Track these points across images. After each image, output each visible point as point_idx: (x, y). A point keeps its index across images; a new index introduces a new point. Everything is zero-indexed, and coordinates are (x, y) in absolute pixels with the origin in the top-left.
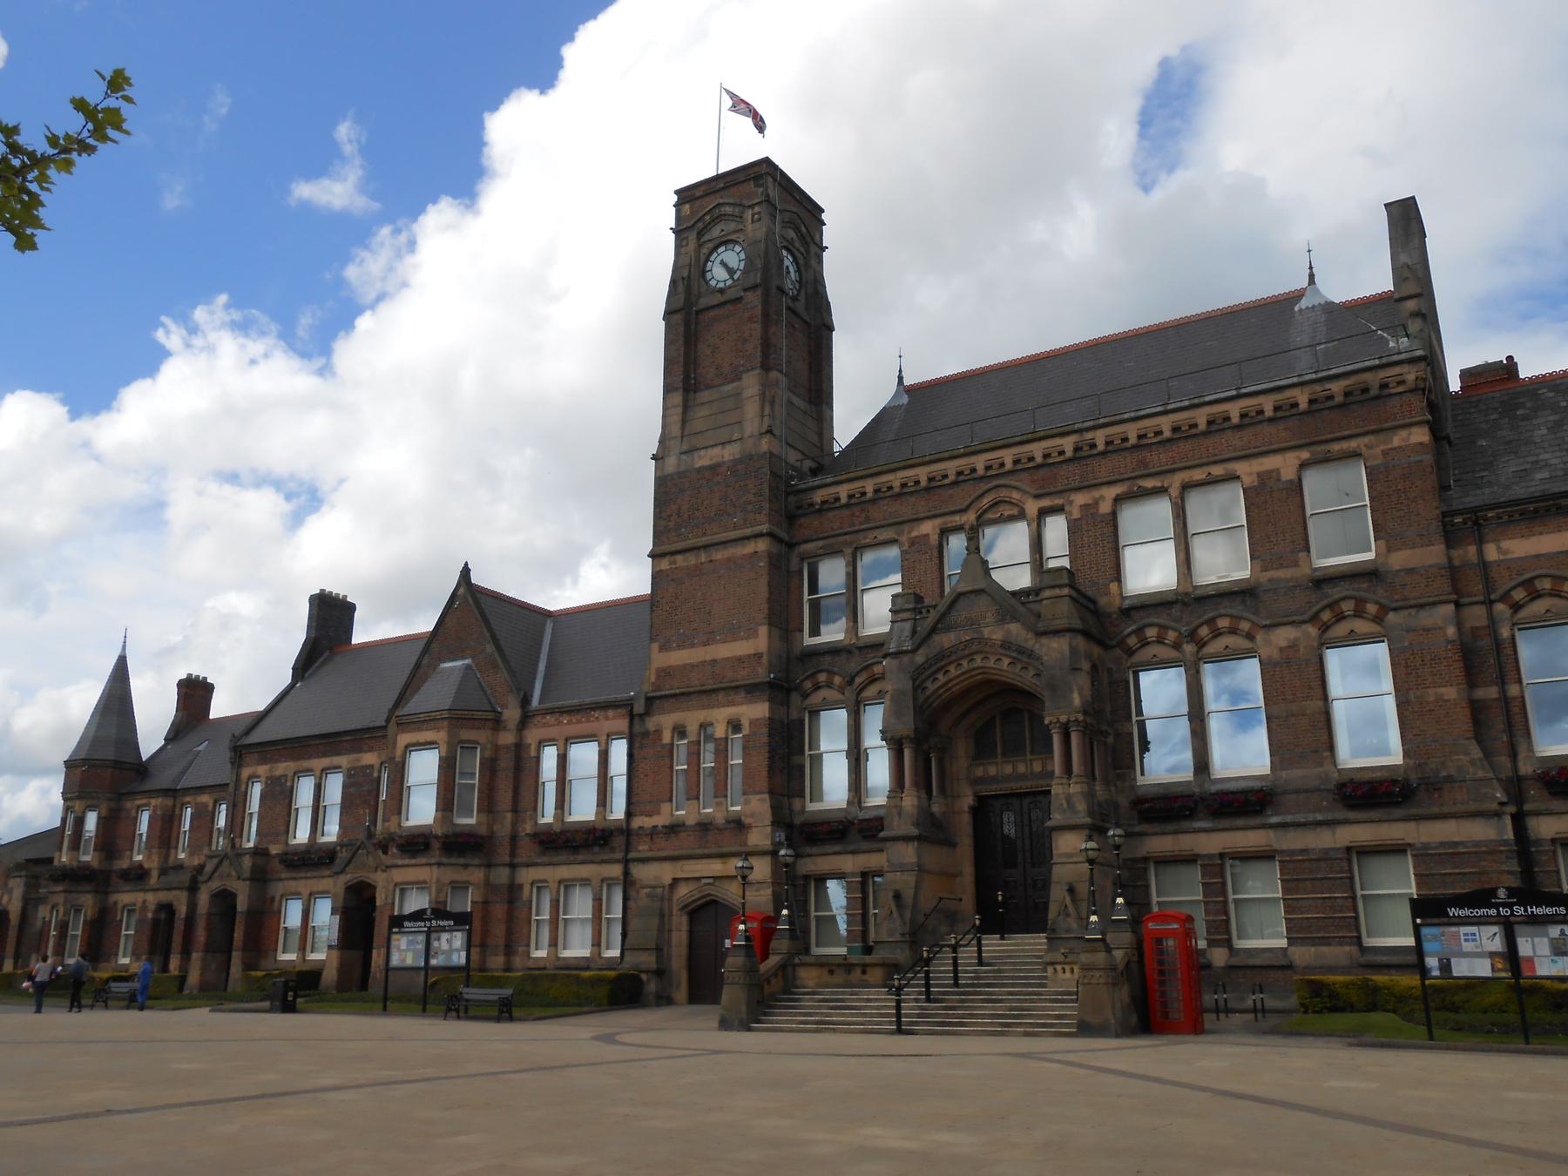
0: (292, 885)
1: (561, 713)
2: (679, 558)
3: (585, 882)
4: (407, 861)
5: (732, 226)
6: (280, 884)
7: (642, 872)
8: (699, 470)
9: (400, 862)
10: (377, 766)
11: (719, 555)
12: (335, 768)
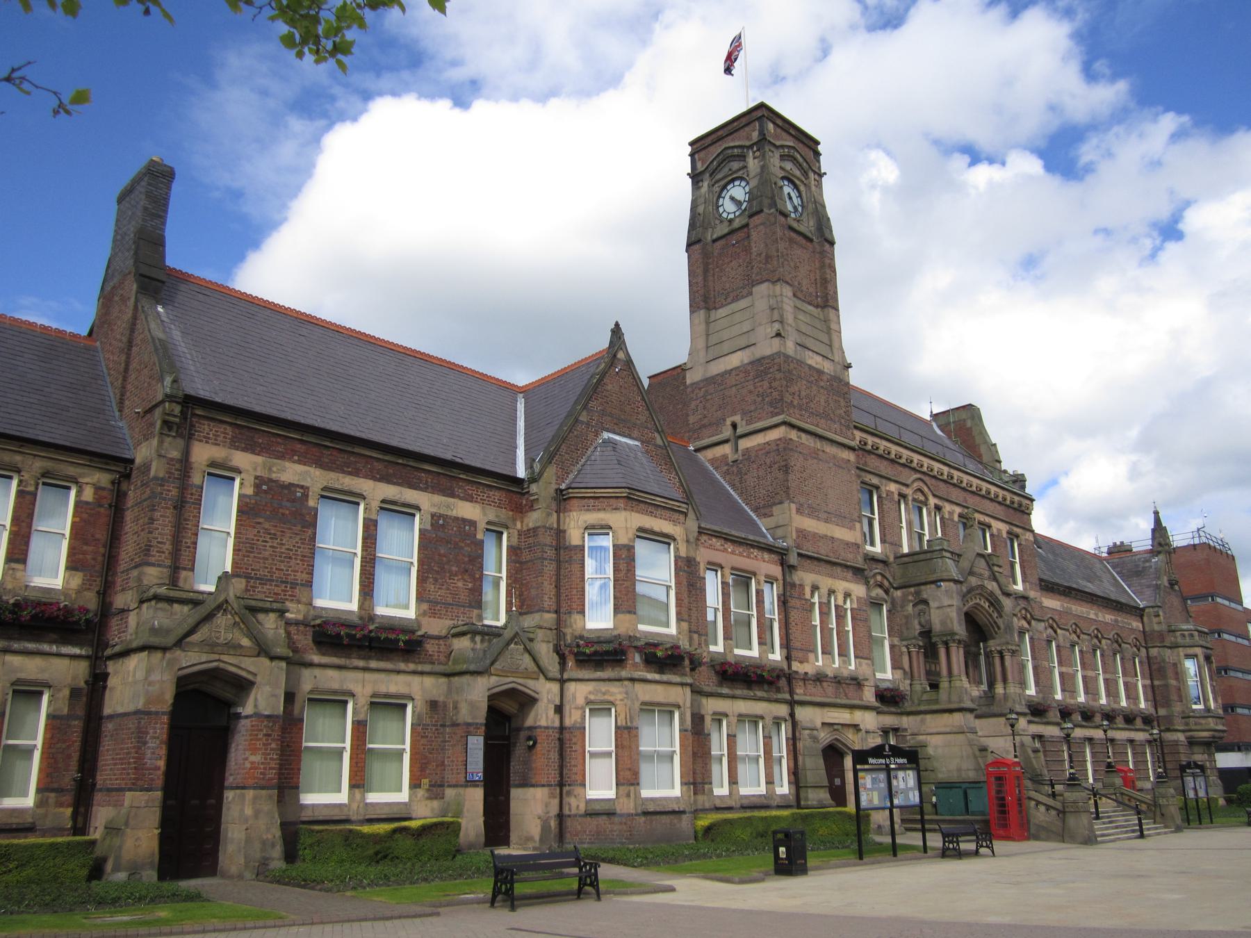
0: (331, 679)
1: (733, 542)
2: (803, 435)
3: (754, 720)
4: (650, 676)
5: (798, 173)
6: (307, 673)
7: (803, 714)
8: (810, 367)
9: (650, 676)
10: (482, 525)
11: (831, 450)
12: (406, 511)
